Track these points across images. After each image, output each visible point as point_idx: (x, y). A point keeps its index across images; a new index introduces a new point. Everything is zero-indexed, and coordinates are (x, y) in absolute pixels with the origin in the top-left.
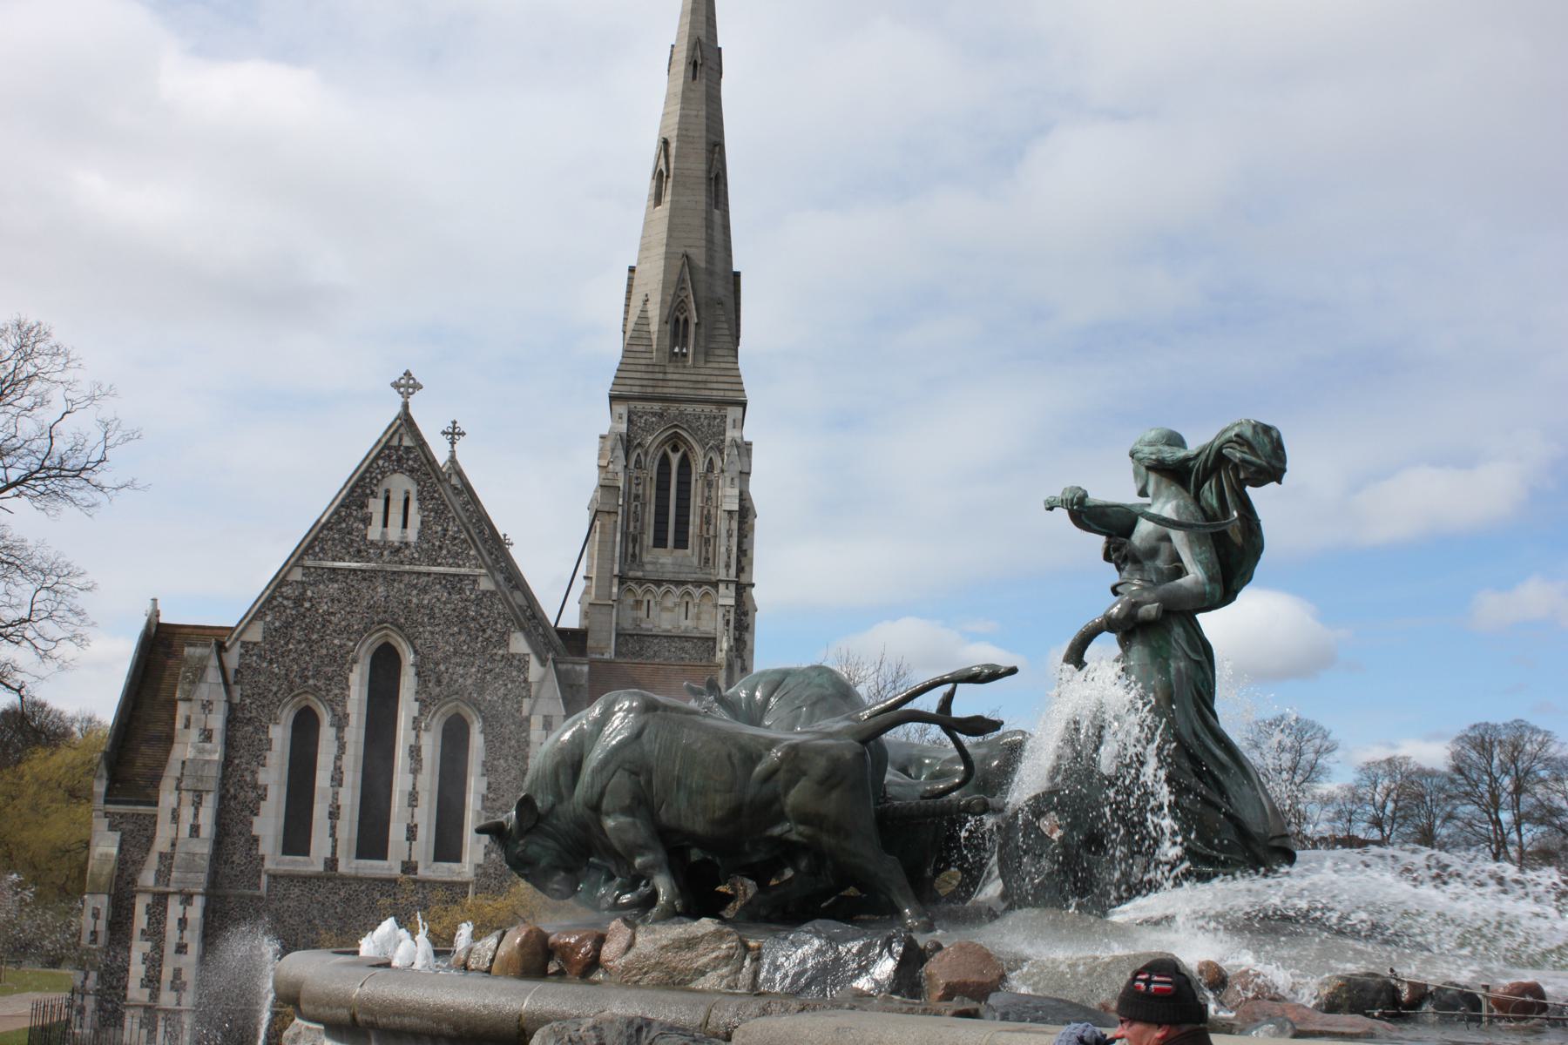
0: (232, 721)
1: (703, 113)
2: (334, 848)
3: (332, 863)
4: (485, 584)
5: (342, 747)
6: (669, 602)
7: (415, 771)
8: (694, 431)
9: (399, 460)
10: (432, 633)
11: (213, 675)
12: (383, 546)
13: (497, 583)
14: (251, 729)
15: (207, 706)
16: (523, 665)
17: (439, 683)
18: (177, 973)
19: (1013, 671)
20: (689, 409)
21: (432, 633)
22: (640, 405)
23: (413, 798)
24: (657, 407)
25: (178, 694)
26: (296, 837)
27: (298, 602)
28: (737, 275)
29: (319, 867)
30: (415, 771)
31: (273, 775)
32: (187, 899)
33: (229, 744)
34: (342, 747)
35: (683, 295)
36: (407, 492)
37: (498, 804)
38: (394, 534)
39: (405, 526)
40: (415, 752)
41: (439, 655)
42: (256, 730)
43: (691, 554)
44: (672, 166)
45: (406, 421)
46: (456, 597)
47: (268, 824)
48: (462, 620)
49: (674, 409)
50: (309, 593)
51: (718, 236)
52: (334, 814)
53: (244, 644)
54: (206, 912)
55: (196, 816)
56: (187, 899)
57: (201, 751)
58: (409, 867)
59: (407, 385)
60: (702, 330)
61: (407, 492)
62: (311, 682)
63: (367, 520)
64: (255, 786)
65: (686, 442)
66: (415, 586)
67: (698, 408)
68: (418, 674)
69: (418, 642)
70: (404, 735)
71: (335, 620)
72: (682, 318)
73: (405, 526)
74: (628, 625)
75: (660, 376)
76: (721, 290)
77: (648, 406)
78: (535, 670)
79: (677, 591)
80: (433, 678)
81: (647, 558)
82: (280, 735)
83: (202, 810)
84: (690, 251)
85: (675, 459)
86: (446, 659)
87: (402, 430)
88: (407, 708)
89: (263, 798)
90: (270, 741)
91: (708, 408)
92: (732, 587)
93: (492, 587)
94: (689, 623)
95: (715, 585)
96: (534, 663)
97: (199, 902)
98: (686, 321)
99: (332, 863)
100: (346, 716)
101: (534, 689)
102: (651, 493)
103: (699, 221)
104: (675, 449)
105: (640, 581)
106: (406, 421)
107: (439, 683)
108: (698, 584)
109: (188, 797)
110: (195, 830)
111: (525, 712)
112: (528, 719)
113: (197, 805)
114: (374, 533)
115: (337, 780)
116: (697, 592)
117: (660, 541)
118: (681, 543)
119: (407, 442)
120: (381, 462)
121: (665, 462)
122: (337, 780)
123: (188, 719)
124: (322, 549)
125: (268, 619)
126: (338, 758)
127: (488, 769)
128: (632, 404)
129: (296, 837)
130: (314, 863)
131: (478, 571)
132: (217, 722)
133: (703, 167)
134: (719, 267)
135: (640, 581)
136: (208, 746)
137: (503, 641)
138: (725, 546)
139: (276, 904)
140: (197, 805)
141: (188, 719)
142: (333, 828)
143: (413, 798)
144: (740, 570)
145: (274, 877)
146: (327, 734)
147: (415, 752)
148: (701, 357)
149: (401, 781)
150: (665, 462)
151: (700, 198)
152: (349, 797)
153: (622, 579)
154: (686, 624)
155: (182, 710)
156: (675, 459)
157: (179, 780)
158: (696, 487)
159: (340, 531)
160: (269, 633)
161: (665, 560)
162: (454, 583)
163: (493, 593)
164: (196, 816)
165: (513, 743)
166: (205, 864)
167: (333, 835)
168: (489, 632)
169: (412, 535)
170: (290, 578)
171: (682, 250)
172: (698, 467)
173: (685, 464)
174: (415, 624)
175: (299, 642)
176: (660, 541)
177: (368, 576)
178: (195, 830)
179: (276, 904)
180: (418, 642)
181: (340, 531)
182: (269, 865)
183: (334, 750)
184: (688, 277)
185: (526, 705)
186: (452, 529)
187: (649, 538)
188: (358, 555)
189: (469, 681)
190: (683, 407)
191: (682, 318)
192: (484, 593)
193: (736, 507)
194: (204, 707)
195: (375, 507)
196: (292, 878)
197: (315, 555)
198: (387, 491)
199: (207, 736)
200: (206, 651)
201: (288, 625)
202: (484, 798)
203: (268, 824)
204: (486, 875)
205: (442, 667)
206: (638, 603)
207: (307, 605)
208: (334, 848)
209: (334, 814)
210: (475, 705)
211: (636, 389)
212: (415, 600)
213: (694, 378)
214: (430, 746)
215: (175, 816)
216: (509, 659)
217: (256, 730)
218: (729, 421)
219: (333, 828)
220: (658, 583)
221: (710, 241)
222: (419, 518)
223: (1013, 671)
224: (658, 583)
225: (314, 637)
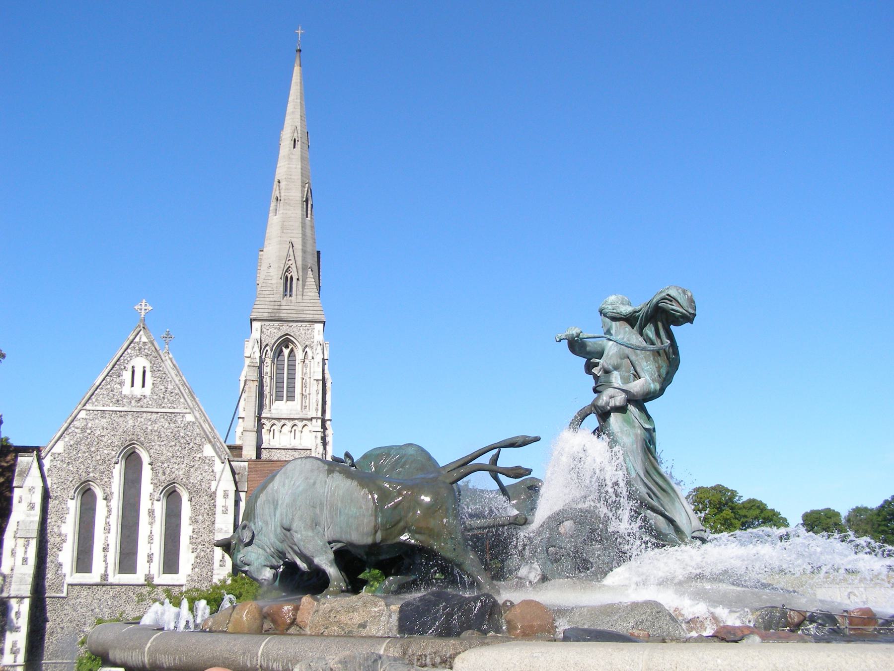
1: (299, 166)
2: (106, 568)
3: (105, 576)
4: (189, 418)
5: (109, 511)
7: (151, 524)
9: (140, 349)
10: (160, 446)
12: (131, 398)
13: (195, 417)
14: (57, 502)
16: (211, 464)
17: (164, 473)
18: (14, 644)
19: (537, 439)
20: (294, 324)
21: (160, 446)
22: (267, 323)
23: (151, 537)
24: (276, 324)
25: (15, 484)
26: (83, 562)
27: (83, 430)
28: (318, 253)
29: (97, 580)
34: (109, 511)
35: (290, 262)
36: (144, 367)
37: (199, 541)
38: (138, 390)
39: (143, 386)
40: (151, 513)
41: (163, 458)
42: (60, 503)
44: (282, 194)
46: (172, 425)
48: (176, 438)
50: (90, 425)
51: (308, 232)
53: (53, 454)
55: (25, 552)
57: (28, 516)
58: (149, 578)
60: (300, 282)
61: (144, 367)
62: (91, 475)
63: (122, 384)
64: (60, 535)
65: (293, 342)
66: (150, 420)
67: (299, 324)
68: (152, 469)
69: (152, 451)
71: (105, 439)
72: (289, 276)
73: (143, 386)
75: (276, 307)
77: (271, 323)
78: (218, 466)
79: (289, 424)
80: (161, 472)
83: (29, 549)
84: (293, 240)
86: (168, 460)
87: (142, 332)
88: (146, 487)
89: (64, 541)
90: (68, 509)
92: (320, 421)
93: (193, 420)
96: (217, 461)
97: (27, 602)
98: (291, 278)
99: (105, 576)
100: (112, 493)
101: (217, 479)
103: (298, 224)
104: (287, 347)
107: (164, 473)
109: (21, 542)
110: (25, 560)
111: (213, 489)
112: (215, 493)
113: (26, 546)
116: (300, 424)
118: (291, 398)
119: (144, 339)
120: (129, 351)
122: (107, 530)
123: (21, 498)
124: (97, 400)
125: (67, 439)
126: (108, 517)
127: (194, 521)
128: (263, 323)
129: (83, 562)
130: (94, 577)
131: (185, 411)
133: (300, 195)
134: (309, 248)
136: (32, 512)
137: (200, 447)
138: (315, 398)
139: (73, 601)
140: (26, 546)
141: (21, 498)
142: (105, 556)
143: (151, 537)
146: (101, 505)
147: (151, 513)
148: (300, 297)
151: (298, 212)
152: (114, 539)
154: (296, 444)
155: (17, 493)
157: (16, 532)
159: (106, 389)
162: (171, 416)
163: (193, 423)
164: (25, 552)
165: (206, 506)
166: (30, 579)
167: (105, 561)
168: (192, 444)
169: (147, 391)
170: (79, 417)
171: (289, 240)
172: (299, 355)
174: (150, 441)
175: (84, 453)
176: (279, 397)
177: (123, 414)
178: (25, 560)
179: (73, 601)
180: (152, 451)
181: (106, 389)
183: (106, 513)
184: (292, 254)
185: (214, 485)
186: (170, 387)
189: (181, 472)
190: (290, 324)
191: (289, 276)
192: (189, 424)
194: (30, 490)
197: (93, 403)
198: (133, 367)
199: (32, 507)
200: (31, 459)
201: (78, 443)
202: (191, 538)
204: (193, 580)
205: (166, 465)
207: (89, 431)
208: (106, 568)
209: (105, 549)
211: (266, 314)
212: (150, 428)
213: (296, 308)
214: (160, 508)
215: (13, 553)
216: (203, 460)
217: (60, 503)
218: (316, 331)
219: (105, 556)
221: (304, 235)
222: (151, 382)
223: (537, 439)
224: (279, 419)
225: (93, 449)
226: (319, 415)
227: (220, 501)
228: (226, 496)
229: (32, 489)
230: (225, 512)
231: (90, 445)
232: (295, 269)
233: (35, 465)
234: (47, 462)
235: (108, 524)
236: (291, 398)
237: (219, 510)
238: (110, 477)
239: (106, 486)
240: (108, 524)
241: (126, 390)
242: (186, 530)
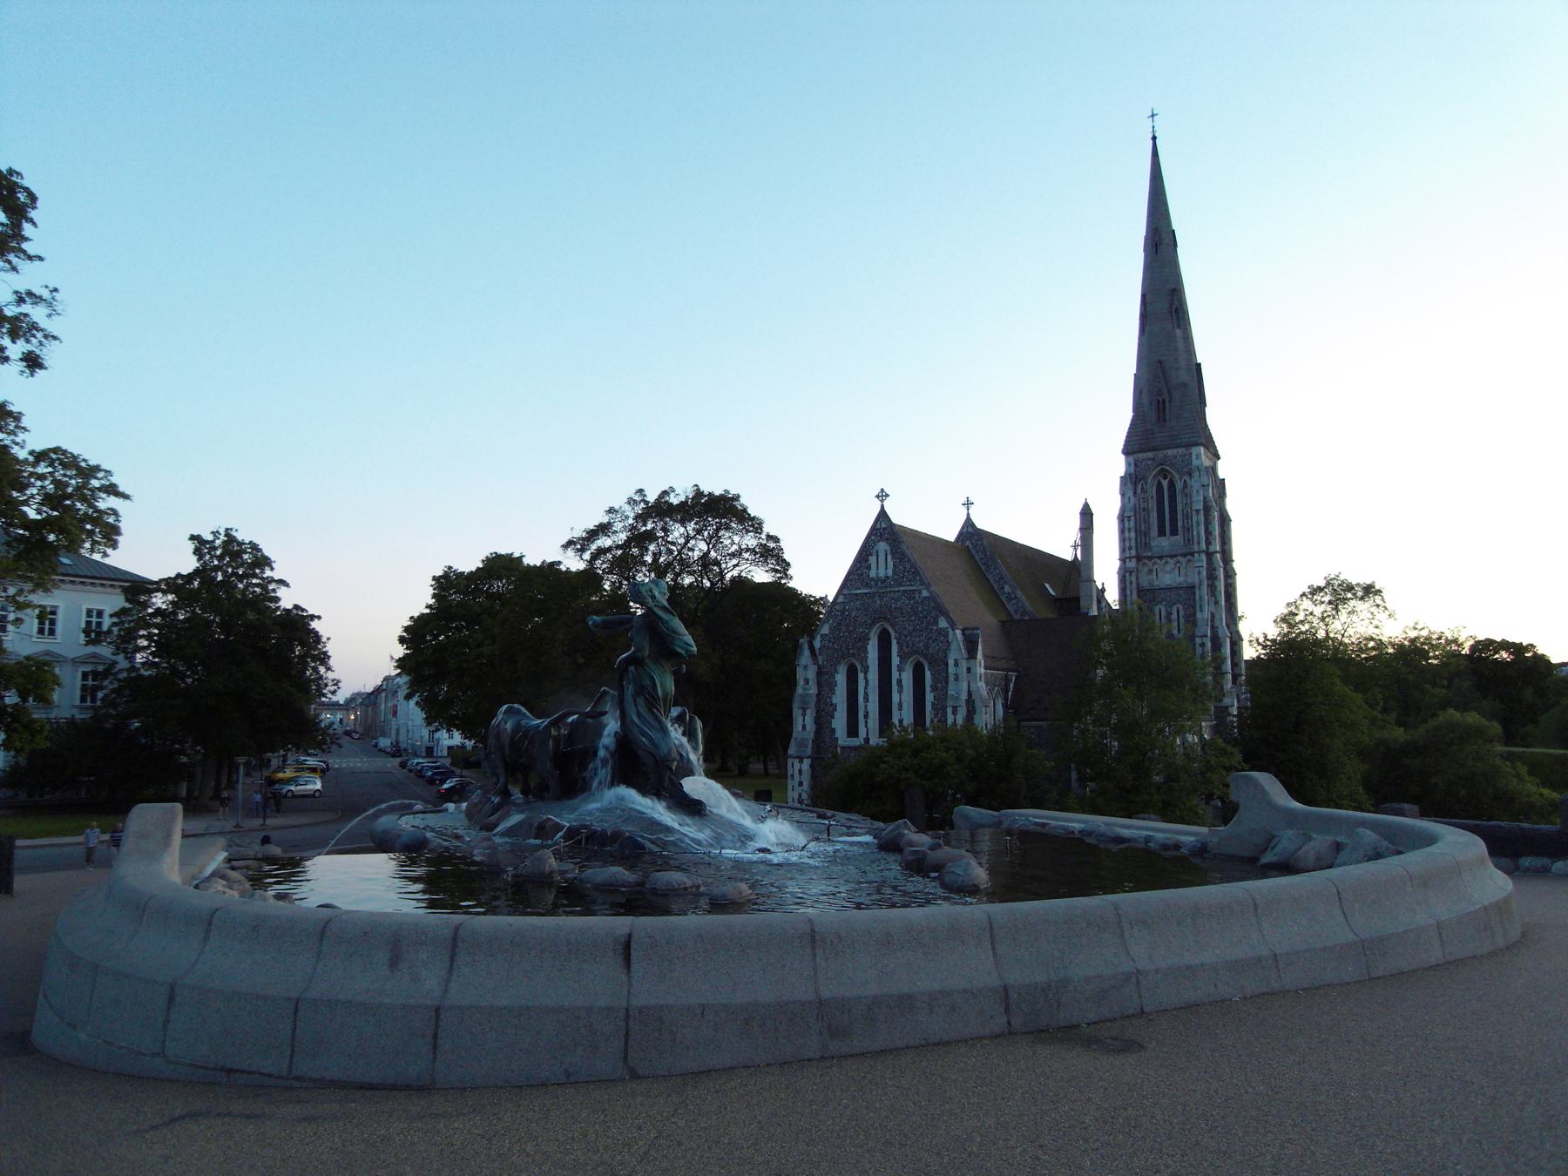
0: (819, 673)
3: (867, 740)
6: (1168, 568)
7: (900, 692)
8: (1172, 465)
11: (806, 652)
12: (879, 579)
15: (806, 667)
16: (946, 636)
20: (1169, 452)
23: (900, 705)
24: (1150, 455)
26: (852, 730)
30: (900, 692)
31: (840, 697)
32: (801, 760)
33: (819, 684)
38: (882, 574)
40: (900, 682)
43: (1179, 538)
45: (883, 515)
47: (839, 722)
49: (1161, 454)
51: (1180, 345)
52: (866, 716)
54: (811, 766)
56: (801, 760)
59: (882, 496)
63: (869, 568)
70: (895, 675)
74: (1145, 583)
76: (1184, 377)
81: (1153, 544)
82: (841, 678)
85: (1165, 483)
86: (910, 633)
88: (895, 660)
91: (1181, 451)
92: (1203, 557)
94: (1182, 579)
95: (1192, 554)
97: (807, 762)
99: (867, 740)
102: (1153, 505)
105: (1150, 558)
106: (883, 515)
108: (1184, 555)
110: (804, 727)
114: (873, 574)
115: (866, 699)
117: (1162, 533)
121: (1160, 486)
122: (866, 699)
127: (934, 688)
129: (852, 730)
132: (811, 674)
135: (1150, 558)
144: (1208, 543)
145: (843, 748)
146: (861, 676)
149: (895, 697)
150: (1160, 486)
152: (873, 707)
153: (1138, 558)
156: (1165, 483)
158: (1179, 498)
160: (832, 629)
161: (1164, 543)
162: (910, 595)
169: (890, 573)
172: (1179, 485)
173: (1172, 485)
176: (1162, 533)
177: (871, 596)
178: (804, 727)
182: (840, 742)
187: (1154, 531)
188: (867, 586)
193: (1201, 506)
195: (872, 560)
196: (851, 748)
203: (839, 722)
206: (1150, 571)
209: (866, 716)
210: (925, 657)
220: (1160, 558)
226: (1203, 546)
227: (951, 669)
228: (956, 664)
229: (806, 667)
230: (957, 679)
231: (848, 626)
232: (1165, 391)
233: (806, 646)
234: (817, 644)
235: (866, 694)
236: (1174, 532)
237: (951, 678)
238: (866, 651)
239: (864, 660)
240: (866, 694)
241: (873, 574)
242: (929, 697)
